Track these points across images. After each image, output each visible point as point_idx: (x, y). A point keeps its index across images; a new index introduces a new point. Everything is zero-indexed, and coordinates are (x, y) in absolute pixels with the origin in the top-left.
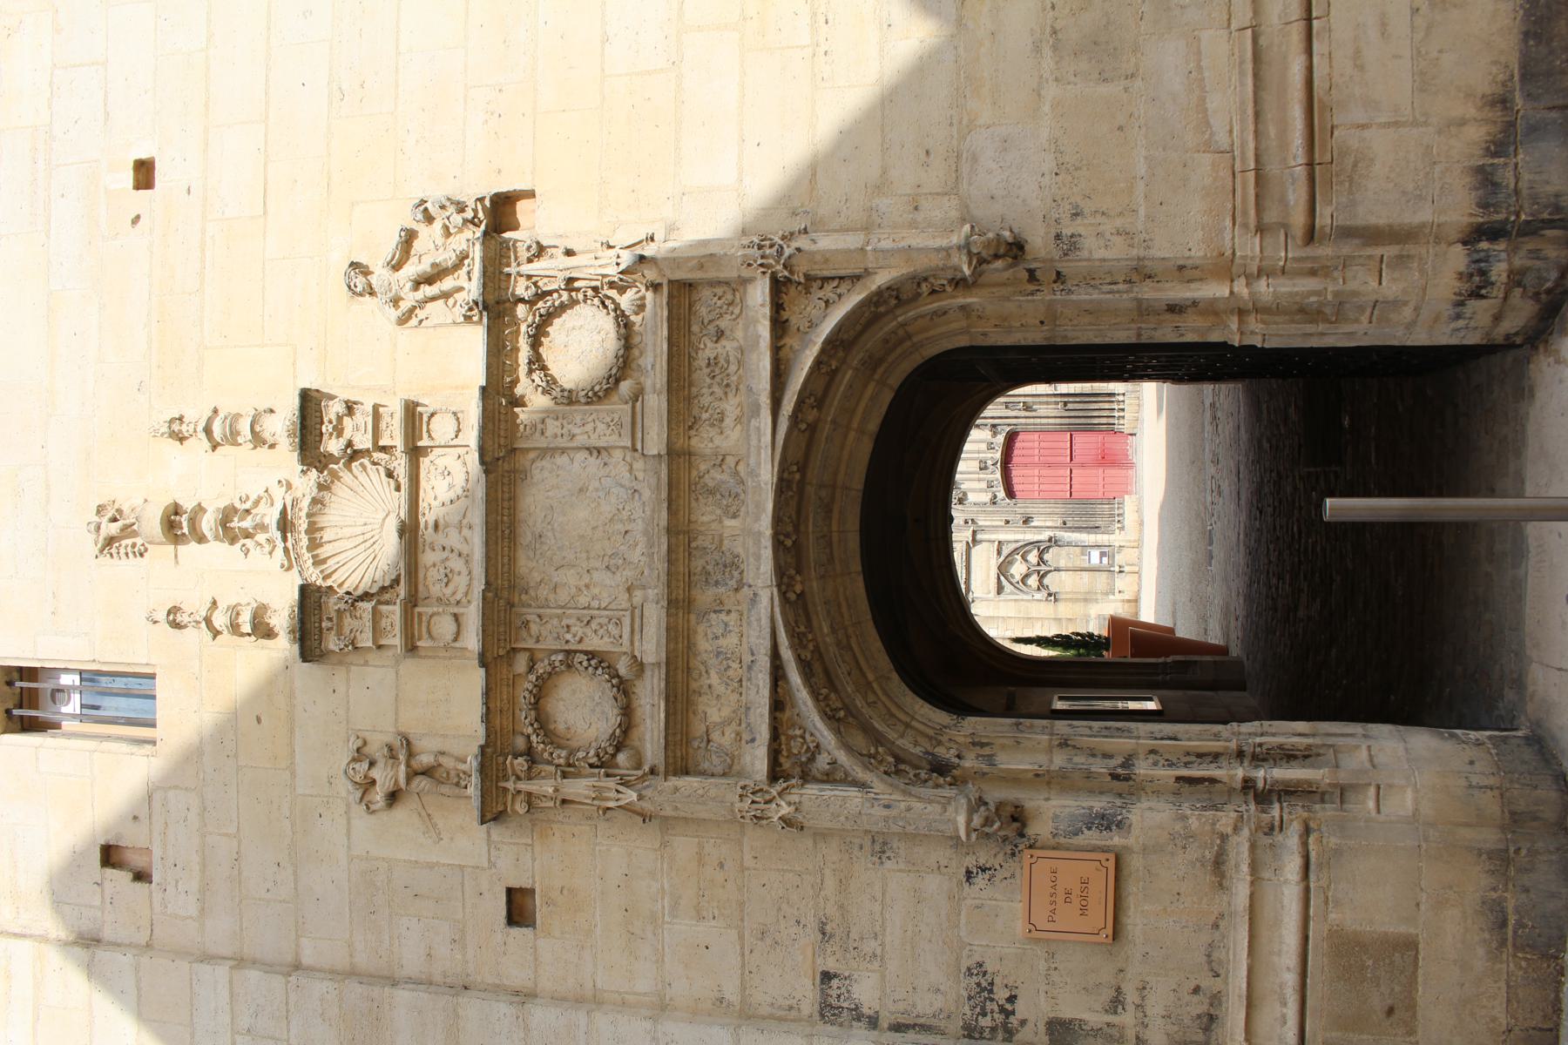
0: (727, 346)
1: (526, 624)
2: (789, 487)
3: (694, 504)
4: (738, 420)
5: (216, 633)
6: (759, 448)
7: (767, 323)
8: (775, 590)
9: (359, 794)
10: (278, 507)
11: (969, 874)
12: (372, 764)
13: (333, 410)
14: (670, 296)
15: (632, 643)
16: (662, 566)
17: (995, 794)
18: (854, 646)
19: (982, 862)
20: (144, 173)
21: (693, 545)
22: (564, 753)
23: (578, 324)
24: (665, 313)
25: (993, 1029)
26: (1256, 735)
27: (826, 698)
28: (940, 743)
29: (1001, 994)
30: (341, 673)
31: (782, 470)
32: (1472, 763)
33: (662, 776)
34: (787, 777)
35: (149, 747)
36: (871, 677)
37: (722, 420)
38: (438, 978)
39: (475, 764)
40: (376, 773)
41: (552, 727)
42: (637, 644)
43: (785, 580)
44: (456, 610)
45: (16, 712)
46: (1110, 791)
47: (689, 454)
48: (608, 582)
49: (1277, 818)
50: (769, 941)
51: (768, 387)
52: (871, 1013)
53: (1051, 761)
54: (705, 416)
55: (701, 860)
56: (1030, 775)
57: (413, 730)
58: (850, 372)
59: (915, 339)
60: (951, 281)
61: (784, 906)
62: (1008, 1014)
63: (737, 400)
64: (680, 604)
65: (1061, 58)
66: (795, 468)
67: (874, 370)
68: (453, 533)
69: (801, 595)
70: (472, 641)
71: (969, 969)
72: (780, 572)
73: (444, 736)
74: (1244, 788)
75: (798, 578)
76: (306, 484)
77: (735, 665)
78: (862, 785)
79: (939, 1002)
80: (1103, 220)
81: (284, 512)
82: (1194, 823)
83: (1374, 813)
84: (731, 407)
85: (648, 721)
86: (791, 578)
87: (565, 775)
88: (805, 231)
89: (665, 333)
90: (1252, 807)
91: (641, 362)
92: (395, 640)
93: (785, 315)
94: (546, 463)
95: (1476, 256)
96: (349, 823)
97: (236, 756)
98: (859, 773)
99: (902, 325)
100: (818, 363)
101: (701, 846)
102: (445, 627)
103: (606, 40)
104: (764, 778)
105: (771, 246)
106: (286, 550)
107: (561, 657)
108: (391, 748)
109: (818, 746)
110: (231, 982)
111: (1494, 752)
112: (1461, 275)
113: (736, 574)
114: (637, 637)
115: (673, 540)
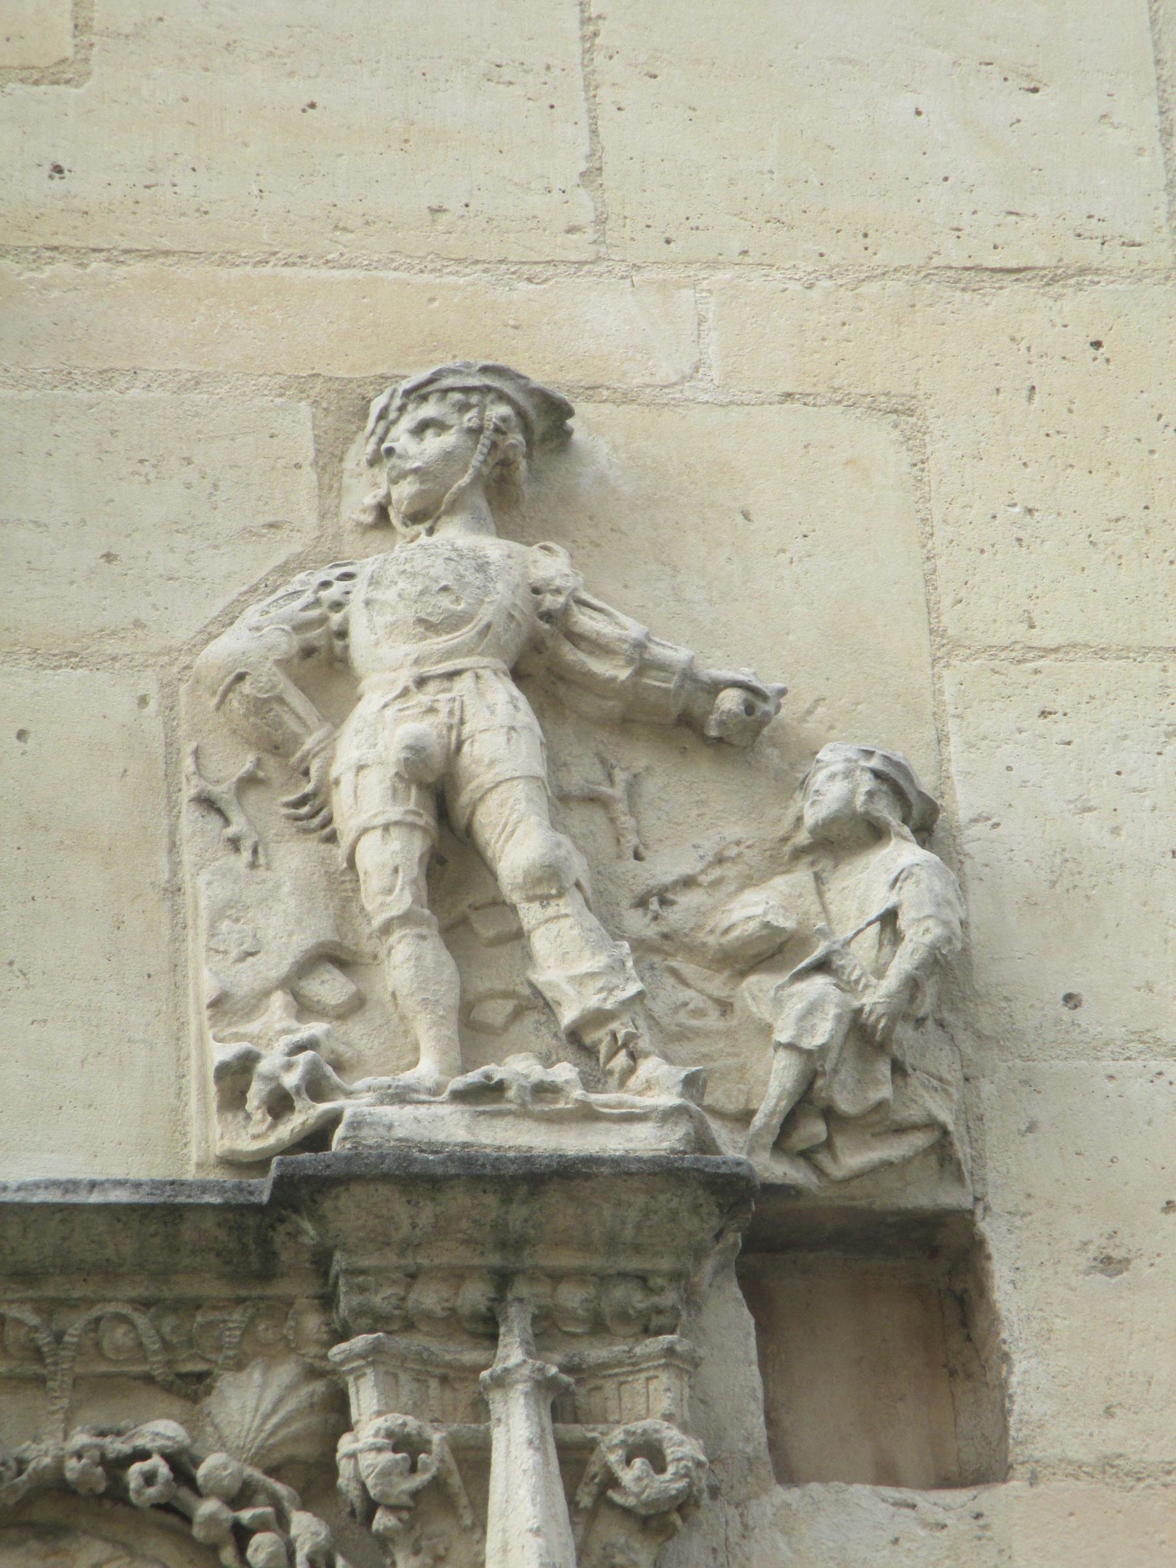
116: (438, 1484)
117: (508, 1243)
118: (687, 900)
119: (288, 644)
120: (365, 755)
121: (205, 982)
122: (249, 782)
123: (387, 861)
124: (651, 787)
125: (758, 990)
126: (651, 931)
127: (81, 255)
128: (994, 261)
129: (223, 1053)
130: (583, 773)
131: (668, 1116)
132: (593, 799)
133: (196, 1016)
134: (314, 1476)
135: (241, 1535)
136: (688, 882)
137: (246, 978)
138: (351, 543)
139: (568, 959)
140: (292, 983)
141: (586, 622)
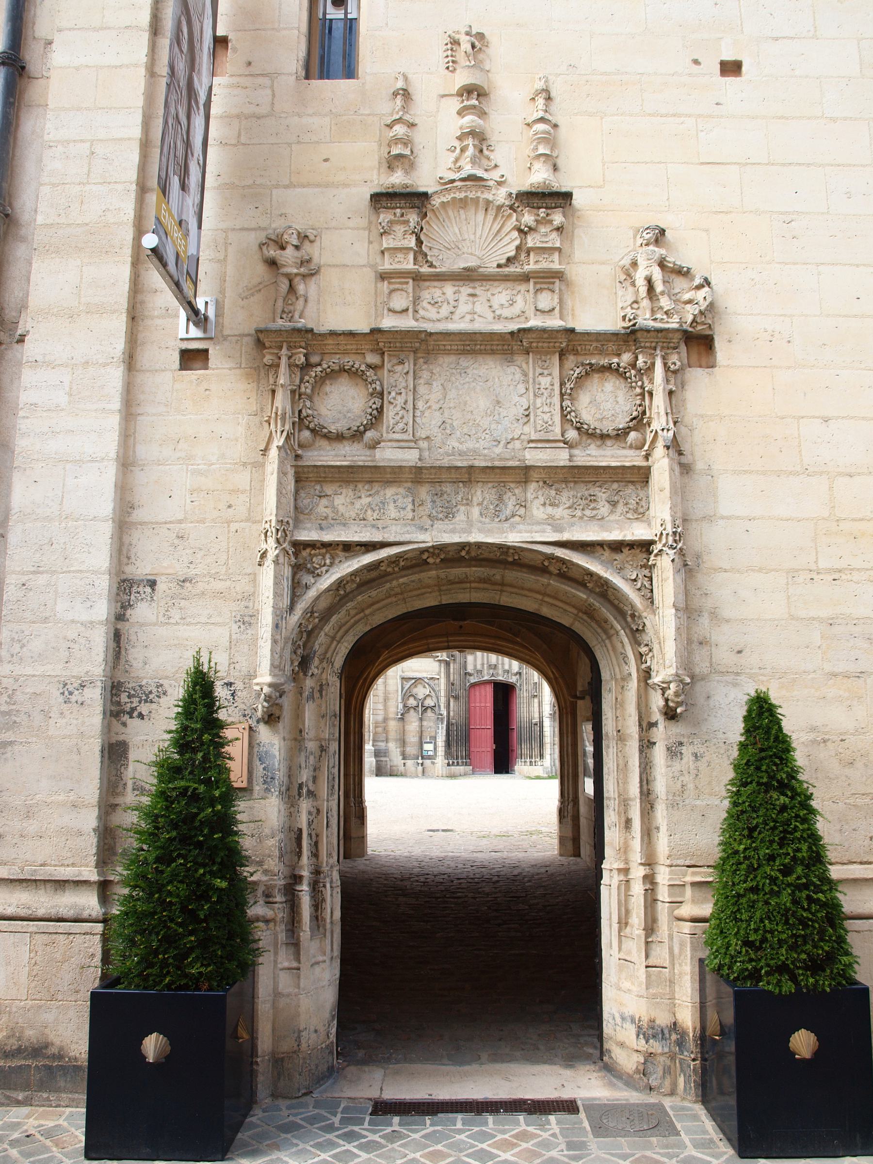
0: (604, 509)
1: (401, 363)
3: (490, 485)
4: (551, 517)
5: (390, 126)
6: (531, 532)
7: (620, 538)
8: (430, 544)
9: (273, 237)
10: (485, 175)
11: (230, 684)
12: (297, 247)
13: (558, 218)
14: (639, 468)
15: (390, 441)
16: (446, 462)
17: (287, 702)
18: (389, 600)
19: (239, 693)
20: (731, 68)
21: (461, 485)
22: (309, 391)
23: (619, 399)
24: (627, 464)
25: (119, 703)
26: (331, 882)
28: (321, 661)
29: (144, 709)
30: (364, 223)
31: (514, 548)
32: (316, 1031)
33: (294, 463)
34: (296, 554)
35: (303, 74)
36: (367, 612)
38: (140, 297)
39: (299, 325)
40: (290, 250)
41: (328, 382)
42: (389, 444)
43: (437, 551)
44: (411, 310)
46: (291, 782)
47: (526, 481)
48: (433, 422)
49: (275, 900)
50: (176, 542)
51: (575, 539)
52: (128, 616)
53: (311, 740)
54: (553, 493)
55: (235, 491)
56: (301, 727)
58: (585, 596)
59: (607, 641)
60: (649, 668)
61: (202, 553)
62: (130, 714)
64: (417, 476)
65: (807, 746)
66: (516, 558)
67: (585, 613)
69: (425, 562)
70: (388, 323)
71: (161, 685)
72: (440, 549)
74: (295, 876)
75: (438, 560)
76: (500, 196)
77: (375, 516)
78: (291, 608)
79: (137, 664)
80: (692, 776)
81: (481, 179)
82: (271, 842)
83: (280, 966)
84: (559, 512)
85: (333, 453)
86: (439, 555)
87: (293, 392)
88: (686, 565)
89: (613, 464)
90: (282, 882)
91: (593, 446)
92: (387, 265)
93: (626, 551)
94: (518, 376)
95: (666, 1032)
97: (299, 142)
99: (617, 633)
102: (400, 301)
103: (826, 420)
105: (675, 541)
107: (378, 388)
108: (309, 261)
109: (318, 575)
110: (129, 139)
111: (324, 1046)
112: (653, 1021)
113: (441, 516)
114: (395, 444)
115: (464, 470)
117: (659, 339)
119: (630, 262)
123: (643, 290)
125: (688, 307)
127: (604, 211)
129: (623, 314)
130: (666, 279)
133: (619, 309)
134: (634, 366)
135: (625, 373)
137: (625, 305)
138: (638, 249)
139: (665, 303)
141: (667, 259)
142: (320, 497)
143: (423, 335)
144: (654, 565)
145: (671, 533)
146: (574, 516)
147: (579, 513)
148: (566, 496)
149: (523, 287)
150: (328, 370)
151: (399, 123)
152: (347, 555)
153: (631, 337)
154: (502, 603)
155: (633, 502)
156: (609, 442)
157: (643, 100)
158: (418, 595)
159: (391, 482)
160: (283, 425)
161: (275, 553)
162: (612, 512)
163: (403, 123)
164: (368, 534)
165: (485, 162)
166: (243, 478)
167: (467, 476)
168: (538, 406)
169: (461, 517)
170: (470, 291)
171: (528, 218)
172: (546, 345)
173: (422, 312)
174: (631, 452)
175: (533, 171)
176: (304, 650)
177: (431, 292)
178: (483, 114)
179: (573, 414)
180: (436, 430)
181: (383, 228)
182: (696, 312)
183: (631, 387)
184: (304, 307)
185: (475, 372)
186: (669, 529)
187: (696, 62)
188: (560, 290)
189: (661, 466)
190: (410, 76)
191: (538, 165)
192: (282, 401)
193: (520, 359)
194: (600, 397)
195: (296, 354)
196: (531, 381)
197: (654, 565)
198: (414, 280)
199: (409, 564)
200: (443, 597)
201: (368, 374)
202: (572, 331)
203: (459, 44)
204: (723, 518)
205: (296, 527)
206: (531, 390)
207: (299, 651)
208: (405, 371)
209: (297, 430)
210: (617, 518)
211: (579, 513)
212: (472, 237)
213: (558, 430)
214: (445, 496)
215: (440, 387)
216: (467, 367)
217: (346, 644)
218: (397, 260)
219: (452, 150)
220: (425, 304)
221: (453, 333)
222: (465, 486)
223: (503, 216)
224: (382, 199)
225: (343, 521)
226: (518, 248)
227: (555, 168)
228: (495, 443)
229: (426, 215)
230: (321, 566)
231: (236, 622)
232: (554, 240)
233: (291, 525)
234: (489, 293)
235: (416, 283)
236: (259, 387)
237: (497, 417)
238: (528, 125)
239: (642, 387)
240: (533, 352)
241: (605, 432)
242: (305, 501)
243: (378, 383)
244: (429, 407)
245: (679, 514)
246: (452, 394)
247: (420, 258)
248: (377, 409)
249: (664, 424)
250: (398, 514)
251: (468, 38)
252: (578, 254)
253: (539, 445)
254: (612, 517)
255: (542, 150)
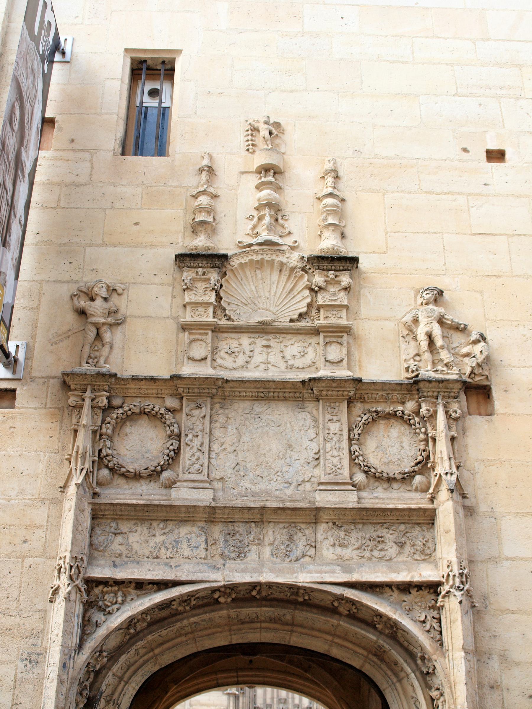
0: (392, 550)
1: (199, 407)
2: (293, 594)
3: (281, 525)
4: (340, 558)
6: (320, 572)
7: (408, 579)
8: (221, 584)
9: (84, 290)
10: (280, 241)
12: (105, 299)
13: (345, 279)
14: (425, 510)
15: (186, 481)
16: (238, 503)
20: (496, 156)
21: (253, 525)
22: (109, 432)
23: (404, 444)
24: (413, 506)
27: (144, 620)
30: (168, 279)
31: (305, 588)
33: (92, 501)
35: (120, 150)
36: (157, 651)
37: (340, 546)
39: (104, 370)
40: (99, 302)
41: (128, 423)
42: (185, 484)
43: (228, 591)
44: (209, 359)
45: (144, 67)
48: (228, 464)
54: (342, 534)
57: (126, 328)
58: (374, 638)
63: (355, 557)
64: (211, 516)
67: (375, 655)
68: (263, 358)
69: (217, 602)
70: (188, 370)
72: (233, 588)
73: (123, 349)
75: (229, 600)
76: (293, 259)
77: (169, 554)
84: (348, 553)
85: (130, 491)
86: (230, 594)
87: (94, 432)
89: (400, 506)
91: (380, 489)
92: (189, 317)
93: (414, 591)
94: (309, 421)
96: (65, 282)
97: (113, 208)
98: (90, 645)
99: (408, 675)
100: (380, 615)
101: (40, 527)
104: (88, 575)
105: (462, 583)
106: (250, 245)
107: (176, 430)
109: (109, 613)
113: (233, 555)
115: (256, 511)
116: (431, 415)
118: (458, 349)
120: (421, 331)
121: (404, 357)
122: (408, 334)
123: (424, 344)
124: (453, 335)
125: (466, 360)
126: (453, 352)
128: (491, 275)
129: (406, 366)
130: (446, 334)
131: (457, 374)
132: (447, 337)
133: (402, 361)
134: (417, 413)
135: (410, 420)
136: (458, 347)
137: (408, 357)
138: (418, 307)
139: (445, 356)
140: (413, 358)
141: (446, 317)
142: (115, 534)
143: (220, 383)
144: (443, 607)
145: (457, 575)
146: (362, 557)
147: (367, 554)
148: (355, 537)
149: (313, 340)
150: (129, 412)
151: (203, 194)
152: (139, 593)
153: (415, 386)
154: (292, 643)
155: (419, 544)
156: (395, 485)
157: (420, 180)
158: (209, 635)
159: (186, 521)
160: (83, 464)
161: (68, 590)
162: (399, 553)
163: (207, 195)
164: (161, 572)
165: (280, 230)
166: (40, 514)
167: (259, 516)
168: (328, 450)
169: (252, 556)
170: (265, 343)
171: (319, 279)
172: (334, 393)
173: (219, 361)
174: (417, 495)
175: (323, 238)
176: (90, 692)
177: (229, 343)
178: (278, 189)
179: (361, 458)
180: (230, 471)
181: (186, 284)
182: (474, 364)
183: (416, 433)
184: (110, 354)
185: (269, 417)
186: (456, 571)
187: (465, 150)
188: (348, 343)
189: (446, 508)
190: (214, 156)
191: (327, 233)
192: (83, 440)
193: (310, 406)
194: (386, 442)
195: (99, 396)
196: (321, 426)
197: (443, 607)
198: (213, 331)
199: (200, 603)
200: (234, 637)
201: (167, 417)
202: (359, 381)
203: (259, 131)
204: (507, 559)
205: (89, 563)
206: (321, 434)
207: (85, 693)
208: (202, 415)
209: (96, 469)
210: (405, 559)
211: (367, 554)
212: (267, 295)
213: (346, 473)
214: (238, 536)
215: (235, 431)
216: (261, 413)
217: (133, 685)
218: (197, 313)
219: (251, 218)
220: (222, 354)
221: (249, 381)
222: (256, 526)
223: (295, 277)
224: (185, 259)
225: (137, 559)
226: (309, 305)
227: (343, 236)
228: (286, 485)
229: (225, 274)
230: (113, 604)
231: (22, 661)
232: (343, 299)
233: (85, 561)
234: (282, 345)
235: (215, 334)
236: (62, 426)
237: (288, 460)
238: (319, 199)
239: (426, 434)
240: (323, 399)
241: (391, 475)
242: (100, 539)
243: (176, 425)
244: (224, 450)
245: (465, 556)
246: (246, 438)
247: (219, 312)
248: (174, 450)
249: (448, 468)
250: (191, 553)
251: (266, 126)
252: (364, 311)
253: (329, 487)
254: (400, 558)
255: (331, 220)
